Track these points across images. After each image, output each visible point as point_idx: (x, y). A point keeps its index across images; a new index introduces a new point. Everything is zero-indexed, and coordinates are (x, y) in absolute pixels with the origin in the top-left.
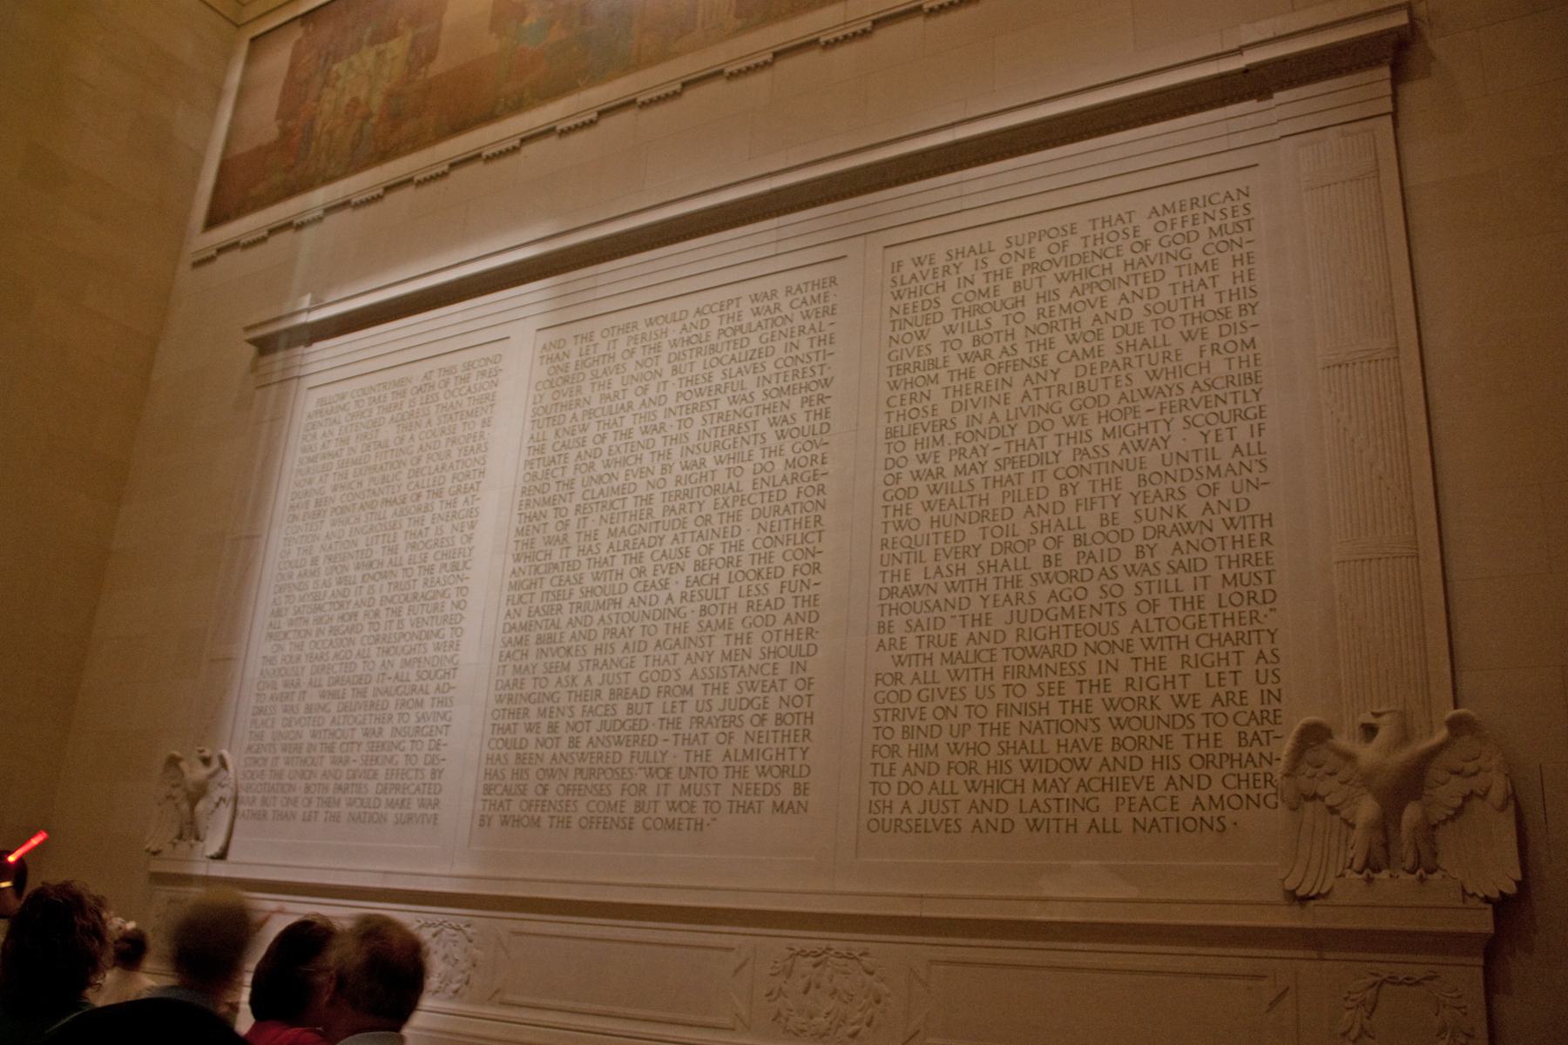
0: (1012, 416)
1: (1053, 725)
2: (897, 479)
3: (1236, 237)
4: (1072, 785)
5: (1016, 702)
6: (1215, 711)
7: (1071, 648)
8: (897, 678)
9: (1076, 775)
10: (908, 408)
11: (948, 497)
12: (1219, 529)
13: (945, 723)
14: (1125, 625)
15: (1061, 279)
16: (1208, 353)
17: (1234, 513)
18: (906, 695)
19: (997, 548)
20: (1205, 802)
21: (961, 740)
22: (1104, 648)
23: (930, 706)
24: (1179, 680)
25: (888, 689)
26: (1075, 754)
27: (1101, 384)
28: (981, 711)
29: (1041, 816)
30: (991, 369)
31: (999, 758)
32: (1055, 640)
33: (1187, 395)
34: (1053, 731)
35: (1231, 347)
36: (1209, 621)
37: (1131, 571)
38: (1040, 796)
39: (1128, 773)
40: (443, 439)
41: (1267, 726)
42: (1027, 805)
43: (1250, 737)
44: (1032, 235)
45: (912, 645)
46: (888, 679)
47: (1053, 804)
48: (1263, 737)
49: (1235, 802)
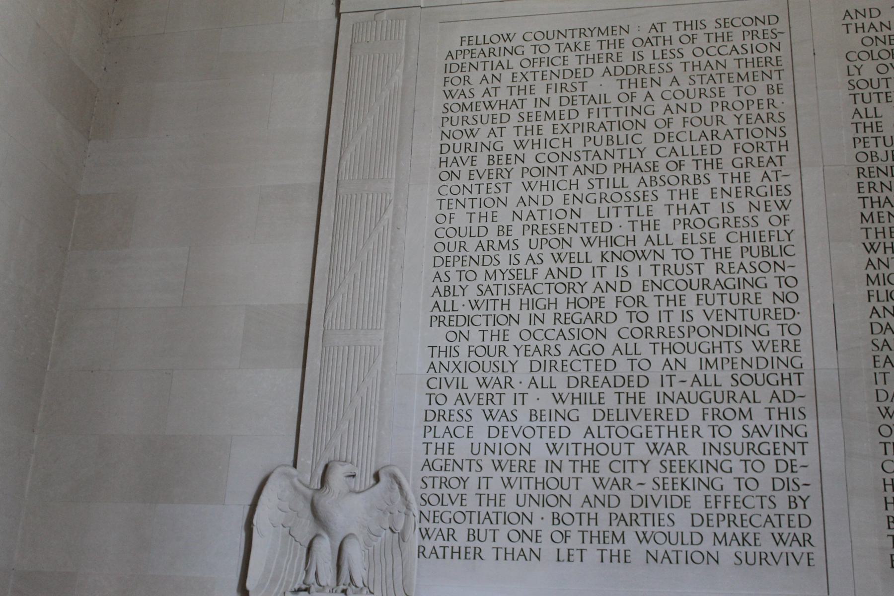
40: (706, 103)
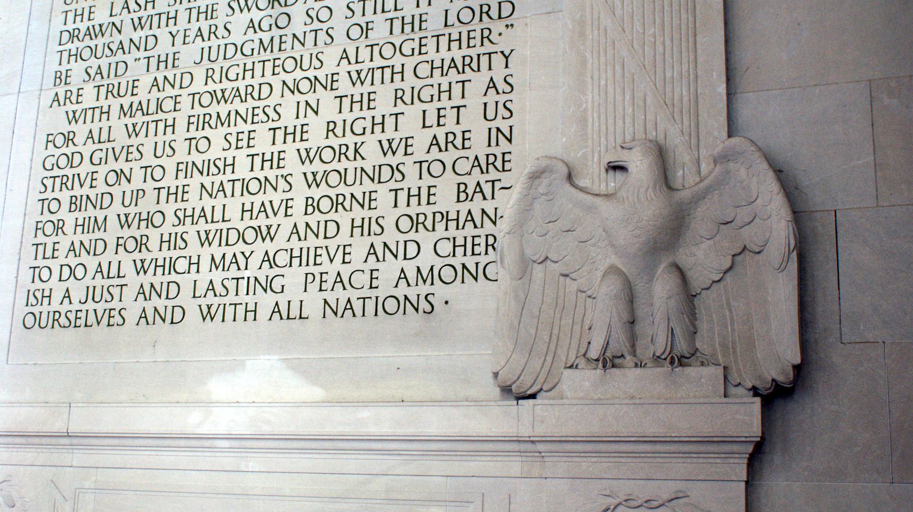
1: (238, 185)
4: (255, 261)
5: (198, 159)
6: (430, 157)
7: (266, 88)
8: (69, 139)
9: (260, 248)
13: (117, 191)
14: (331, 56)
18: (77, 158)
20: (411, 275)
21: (132, 210)
22: (305, 86)
23: (103, 170)
24: (390, 122)
25: (57, 152)
26: (262, 221)
28: (158, 173)
29: (217, 301)
31: (173, 230)
34: (238, 191)
36: (431, 44)
38: (217, 276)
39: (321, 242)
41: (493, 174)
43: (470, 191)
45: (89, 98)
46: (60, 140)
47: (231, 285)
48: (487, 188)
49: (448, 274)
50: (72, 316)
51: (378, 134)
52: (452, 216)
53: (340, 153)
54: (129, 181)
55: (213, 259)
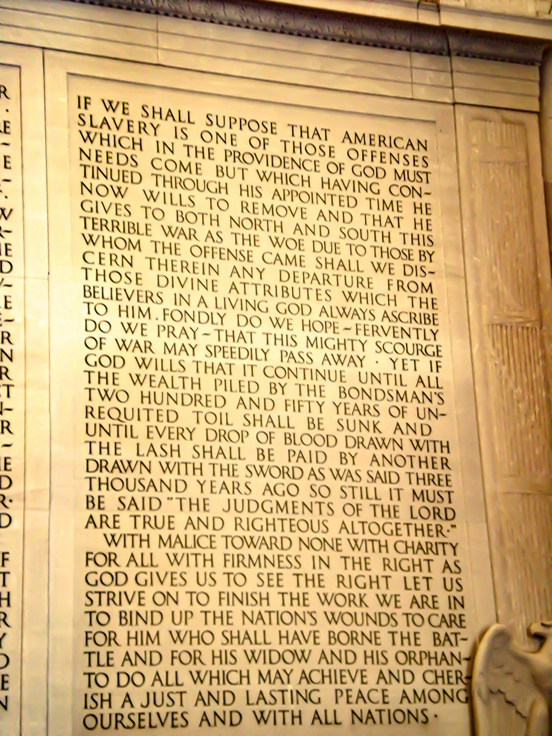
0: (221, 304)
1: (274, 616)
2: (100, 344)
3: (417, 186)
8: (110, 559)
9: (297, 668)
10: (109, 269)
11: (158, 375)
12: (408, 450)
13: (166, 610)
14: (334, 523)
15: (263, 177)
16: (394, 287)
17: (419, 436)
19: (212, 435)
20: (411, 695)
23: (149, 591)
24: (382, 581)
25: (100, 570)
26: (296, 646)
27: (304, 293)
29: (267, 708)
30: (196, 251)
31: (224, 648)
32: (271, 533)
33: (378, 322)
35: (413, 287)
36: (403, 530)
37: (337, 475)
38: (266, 688)
39: (343, 666)
41: (455, 629)
42: (253, 698)
43: (442, 638)
44: (232, 121)
46: (101, 560)
47: (278, 695)
48: (452, 638)
50: (135, 718)
51: (375, 590)
52: (433, 655)
53: (350, 601)
54: (176, 602)
55: (260, 674)
